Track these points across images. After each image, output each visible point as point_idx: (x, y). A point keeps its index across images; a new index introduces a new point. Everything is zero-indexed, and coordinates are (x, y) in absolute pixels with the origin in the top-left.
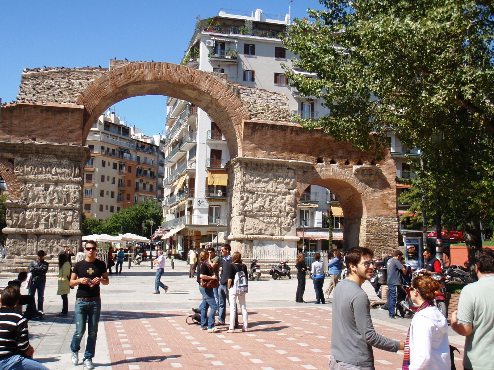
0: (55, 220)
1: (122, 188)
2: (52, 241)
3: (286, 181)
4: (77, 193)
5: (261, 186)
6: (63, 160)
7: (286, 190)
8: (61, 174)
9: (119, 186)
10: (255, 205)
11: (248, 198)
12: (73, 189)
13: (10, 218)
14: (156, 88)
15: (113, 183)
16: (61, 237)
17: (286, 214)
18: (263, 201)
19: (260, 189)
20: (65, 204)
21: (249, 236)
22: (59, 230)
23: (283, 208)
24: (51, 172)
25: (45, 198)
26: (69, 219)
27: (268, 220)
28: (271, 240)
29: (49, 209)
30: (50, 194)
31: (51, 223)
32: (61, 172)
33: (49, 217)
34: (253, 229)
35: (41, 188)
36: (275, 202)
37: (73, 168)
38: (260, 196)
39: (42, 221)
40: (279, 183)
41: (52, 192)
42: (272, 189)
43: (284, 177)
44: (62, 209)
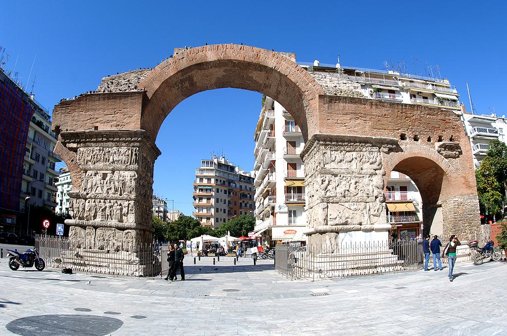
4: (133, 181)
7: (373, 171)
12: (129, 178)
13: (72, 209)
14: (223, 76)
17: (374, 198)
18: (348, 184)
20: (121, 195)
23: (371, 192)
25: (102, 187)
26: (125, 210)
27: (355, 207)
30: (107, 183)
34: (338, 219)
35: (99, 177)
36: (361, 185)
38: (345, 178)
39: (99, 214)
41: (108, 182)
44: (116, 199)
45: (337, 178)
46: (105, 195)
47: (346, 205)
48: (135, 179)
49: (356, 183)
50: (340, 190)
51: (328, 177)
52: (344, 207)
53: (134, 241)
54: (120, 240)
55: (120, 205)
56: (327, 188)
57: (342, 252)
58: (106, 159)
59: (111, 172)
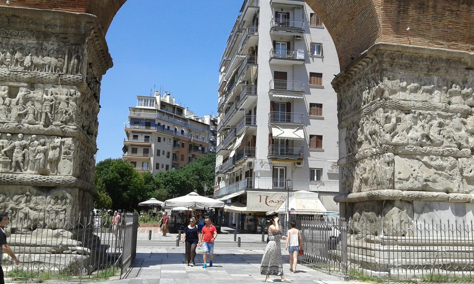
0: (24, 155)
1: (175, 162)
2: (16, 197)
3: (465, 91)
4: (71, 102)
5: (420, 99)
6: (47, 41)
7: (467, 107)
8: (41, 67)
9: (173, 160)
10: (412, 134)
11: (399, 120)
12: (64, 97)
15: (168, 157)
16: (35, 191)
17: (469, 151)
18: (426, 125)
19: (419, 104)
20: (46, 125)
21: (405, 193)
22: (31, 176)
24: (23, 62)
27: (439, 162)
28: (447, 200)
29: (14, 134)
30: (17, 104)
31: (17, 162)
32: (42, 62)
33: (12, 150)
34: (411, 180)
36: (447, 128)
37: (66, 57)
38: (421, 117)
40: (452, 95)
41: (21, 101)
42: (440, 104)
43: (461, 83)
45: (408, 117)
46: (13, 125)
47: (425, 159)
48: (75, 100)
49: (441, 125)
50: (416, 133)
51: (394, 115)
52: (421, 162)
53: (69, 210)
54: (40, 207)
55: (44, 145)
56: (394, 129)
57: (418, 237)
58: (17, 61)
59: (26, 85)
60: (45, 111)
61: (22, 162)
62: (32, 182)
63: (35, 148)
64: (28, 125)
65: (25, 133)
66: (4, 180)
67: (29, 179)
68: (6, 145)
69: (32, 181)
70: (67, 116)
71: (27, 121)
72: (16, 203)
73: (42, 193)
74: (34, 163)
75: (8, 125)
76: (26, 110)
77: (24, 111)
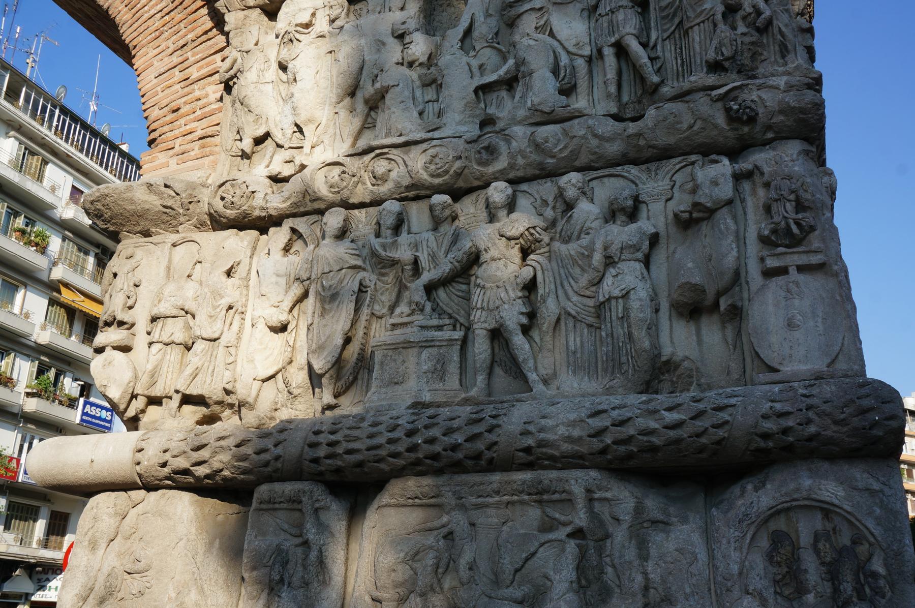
41: (483, 29)
60: (613, 40)
61: (526, 330)
62: (596, 444)
63: (585, 240)
64: (533, 129)
65: (520, 174)
66: (431, 441)
67: (572, 424)
68: (433, 257)
69: (599, 433)
70: (742, 28)
71: (522, 113)
72: (518, 594)
73: (672, 510)
74: (590, 326)
75: (432, 152)
76: (511, 62)
77: (502, 72)
